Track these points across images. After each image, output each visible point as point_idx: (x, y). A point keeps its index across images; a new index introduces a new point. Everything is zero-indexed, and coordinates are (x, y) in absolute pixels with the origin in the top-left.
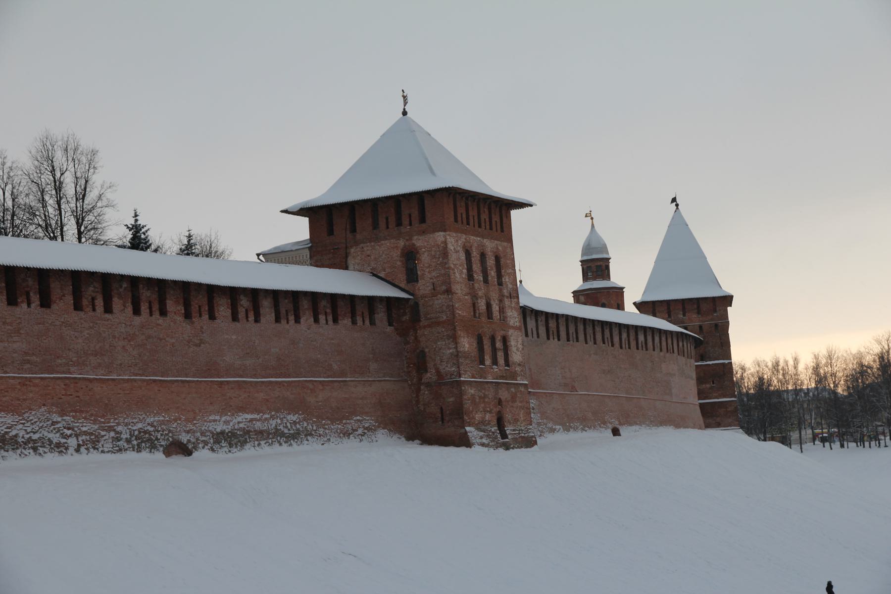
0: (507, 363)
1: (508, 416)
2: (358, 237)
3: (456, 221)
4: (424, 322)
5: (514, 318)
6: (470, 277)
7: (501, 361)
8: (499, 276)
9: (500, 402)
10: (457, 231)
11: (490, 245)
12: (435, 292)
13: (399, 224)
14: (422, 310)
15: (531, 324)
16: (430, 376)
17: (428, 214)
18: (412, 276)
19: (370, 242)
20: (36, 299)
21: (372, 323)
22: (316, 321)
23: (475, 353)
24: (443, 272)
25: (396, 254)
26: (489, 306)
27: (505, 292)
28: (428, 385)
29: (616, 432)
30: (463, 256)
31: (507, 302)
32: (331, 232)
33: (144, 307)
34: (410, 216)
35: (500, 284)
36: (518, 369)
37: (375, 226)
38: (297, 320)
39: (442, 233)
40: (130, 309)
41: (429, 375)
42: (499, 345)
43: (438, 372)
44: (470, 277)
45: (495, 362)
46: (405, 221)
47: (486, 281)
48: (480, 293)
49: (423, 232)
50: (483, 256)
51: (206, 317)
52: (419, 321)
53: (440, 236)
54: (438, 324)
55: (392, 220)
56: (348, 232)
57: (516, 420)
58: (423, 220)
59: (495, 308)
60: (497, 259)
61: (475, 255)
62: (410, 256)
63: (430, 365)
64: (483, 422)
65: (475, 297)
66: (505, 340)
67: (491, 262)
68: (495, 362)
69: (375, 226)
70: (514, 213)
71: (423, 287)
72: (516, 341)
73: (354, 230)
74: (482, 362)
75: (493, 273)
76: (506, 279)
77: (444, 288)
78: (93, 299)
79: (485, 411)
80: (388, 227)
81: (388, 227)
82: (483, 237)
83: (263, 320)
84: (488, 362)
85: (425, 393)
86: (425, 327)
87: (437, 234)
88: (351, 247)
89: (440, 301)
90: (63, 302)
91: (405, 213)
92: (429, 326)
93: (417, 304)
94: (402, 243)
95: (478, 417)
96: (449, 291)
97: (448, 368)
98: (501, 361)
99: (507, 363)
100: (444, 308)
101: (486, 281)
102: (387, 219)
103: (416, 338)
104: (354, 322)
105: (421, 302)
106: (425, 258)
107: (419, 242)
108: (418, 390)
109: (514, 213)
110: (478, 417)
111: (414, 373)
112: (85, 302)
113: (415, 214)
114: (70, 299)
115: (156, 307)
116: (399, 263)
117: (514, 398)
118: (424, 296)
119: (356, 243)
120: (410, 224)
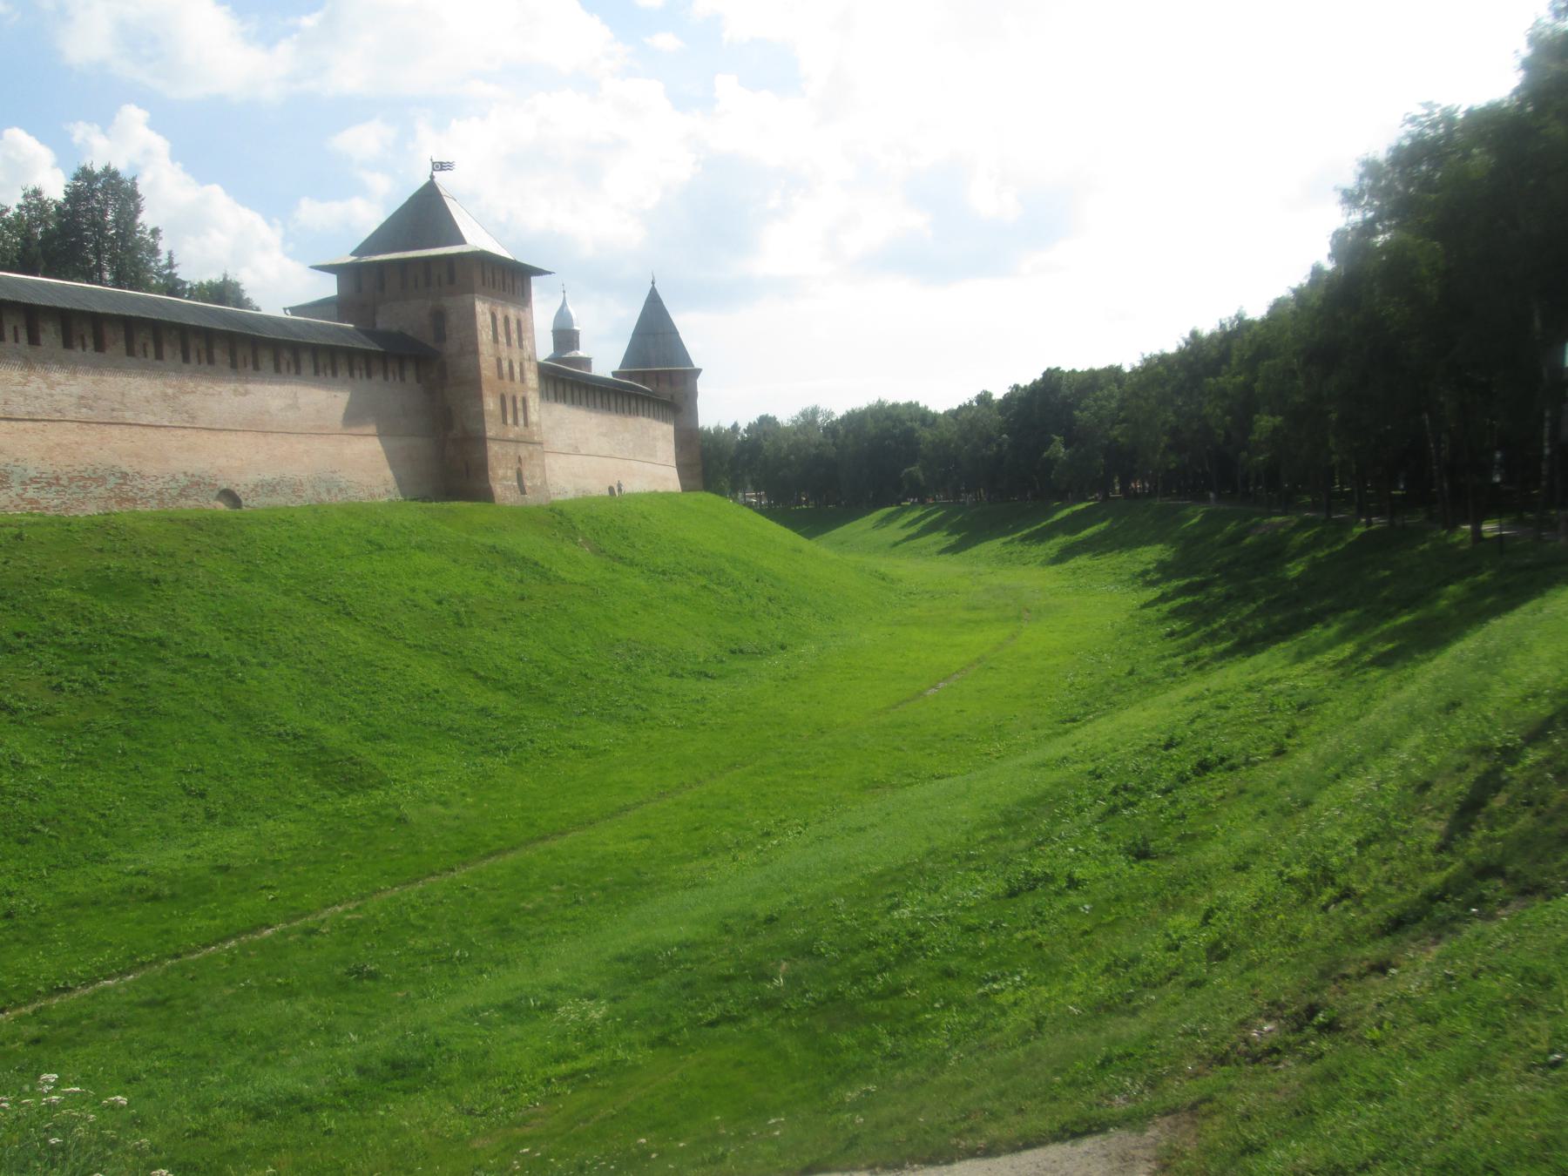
0: (526, 424)
1: (526, 473)
5: (532, 379)
6: (496, 339)
7: (521, 421)
8: (520, 339)
11: (512, 313)
18: (441, 336)
20: (90, 342)
21: (402, 379)
23: (498, 412)
31: (526, 365)
33: (193, 355)
35: (521, 346)
40: (179, 356)
42: (519, 405)
44: (496, 339)
47: (509, 343)
48: (504, 355)
50: (507, 320)
51: (250, 367)
59: (517, 369)
60: (519, 323)
61: (500, 317)
62: (439, 317)
64: (505, 478)
65: (499, 361)
66: (524, 401)
67: (513, 326)
68: (516, 423)
70: (534, 279)
72: (534, 401)
74: (505, 422)
75: (514, 336)
76: (526, 343)
78: (145, 345)
84: (510, 420)
98: (521, 421)
99: (526, 424)
101: (509, 343)
104: (386, 378)
109: (534, 279)
110: (501, 472)
112: (137, 347)
114: (122, 344)
115: (204, 356)
117: (531, 455)
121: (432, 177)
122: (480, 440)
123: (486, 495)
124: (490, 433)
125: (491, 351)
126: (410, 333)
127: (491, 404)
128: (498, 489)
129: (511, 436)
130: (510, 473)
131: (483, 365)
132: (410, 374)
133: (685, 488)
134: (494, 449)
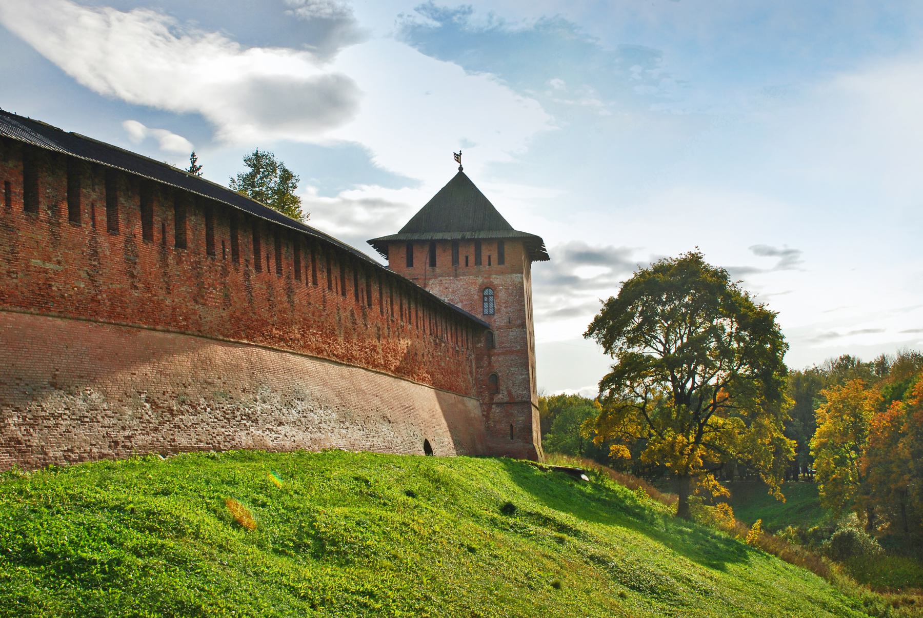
2: (438, 270)
4: (498, 350)
12: (510, 324)
13: (478, 262)
14: (497, 339)
16: (501, 397)
17: (507, 258)
19: (449, 276)
24: (518, 308)
25: (474, 289)
28: (499, 404)
32: (410, 263)
34: (489, 257)
37: (455, 261)
39: (519, 275)
41: (500, 396)
43: (510, 393)
46: (485, 259)
52: (493, 347)
55: (472, 259)
56: (428, 266)
58: (501, 261)
63: (503, 387)
69: (455, 261)
70: (536, 265)
73: (433, 264)
77: (519, 322)
80: (467, 265)
81: (467, 265)
86: (499, 355)
87: (514, 275)
88: (430, 279)
91: (485, 252)
92: (503, 354)
93: (491, 334)
94: (480, 280)
100: (519, 339)
102: (467, 258)
103: (490, 363)
105: (496, 333)
106: (502, 295)
107: (497, 280)
108: (489, 409)
111: (486, 394)
113: (495, 257)
116: (476, 297)
118: (500, 328)
119: (435, 277)
120: (490, 265)
121: (461, 169)
126: (459, 306)
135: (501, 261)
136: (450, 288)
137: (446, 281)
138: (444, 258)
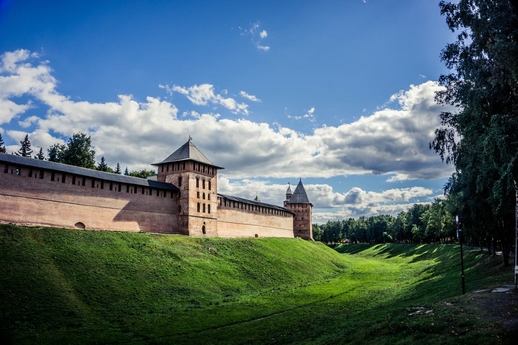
3: (194, 169)
4: (181, 198)
5: (214, 198)
6: (198, 186)
9: (204, 223)
10: (194, 172)
13: (178, 169)
15: (228, 203)
16: (181, 213)
18: (180, 185)
22: (143, 193)
25: (177, 178)
26: (204, 194)
27: (212, 192)
28: (181, 216)
29: (256, 236)
30: (195, 180)
31: (211, 195)
32: (162, 171)
35: (210, 189)
36: (214, 214)
37: (173, 170)
38: (135, 192)
42: (206, 206)
44: (198, 186)
45: (204, 211)
47: (204, 187)
49: (184, 172)
53: (188, 173)
54: (185, 198)
57: (210, 229)
58: (184, 169)
62: (180, 179)
63: (182, 210)
66: (209, 205)
68: (204, 211)
69: (173, 170)
71: (182, 188)
73: (168, 171)
74: (199, 211)
79: (198, 225)
82: (205, 175)
83: (122, 191)
85: (180, 217)
89: (185, 192)
90: (139, 191)
91: (180, 166)
94: (178, 175)
95: (194, 226)
96: (188, 189)
97: (185, 211)
101: (204, 187)
107: (183, 175)
114: (50, 177)
117: (210, 222)
119: (168, 174)
122: (187, 216)
123: (187, 233)
124: (190, 214)
125: (195, 190)
127: (192, 205)
128: (191, 231)
129: (201, 216)
130: (199, 227)
131: (190, 192)
132: (169, 195)
133: (295, 236)
134: (191, 219)
135: (184, 169)
136: (171, 179)
137: (170, 176)
138: (170, 169)
